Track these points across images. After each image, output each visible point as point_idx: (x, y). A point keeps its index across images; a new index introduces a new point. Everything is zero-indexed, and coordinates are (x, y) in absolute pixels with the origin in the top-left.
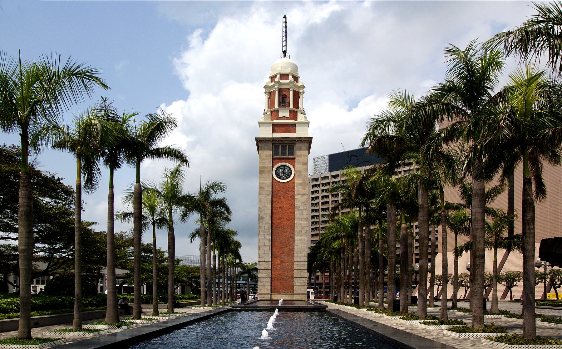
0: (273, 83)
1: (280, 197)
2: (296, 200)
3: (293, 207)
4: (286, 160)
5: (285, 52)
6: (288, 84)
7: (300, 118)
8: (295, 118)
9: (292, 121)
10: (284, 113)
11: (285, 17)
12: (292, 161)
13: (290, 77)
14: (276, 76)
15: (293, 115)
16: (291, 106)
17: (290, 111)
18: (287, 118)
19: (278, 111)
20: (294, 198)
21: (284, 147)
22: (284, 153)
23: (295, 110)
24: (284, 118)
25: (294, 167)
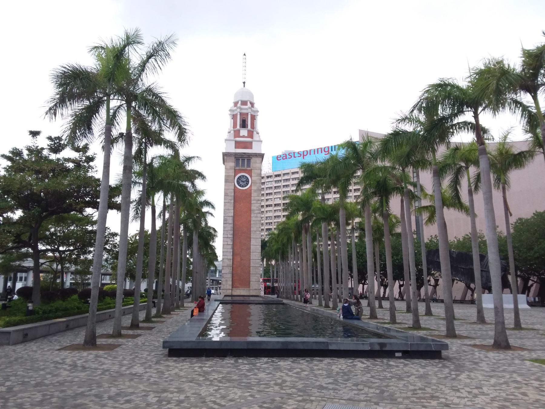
0: (236, 108)
1: (240, 202)
2: (252, 205)
3: (249, 211)
4: (245, 171)
5: (244, 83)
6: (246, 109)
7: (256, 137)
8: (252, 137)
9: (249, 139)
10: (244, 132)
11: (245, 55)
12: (250, 172)
13: (249, 103)
14: (238, 102)
15: (251, 134)
17: (249, 131)
19: (239, 131)
20: (251, 203)
22: (243, 165)
23: (252, 130)
24: (244, 137)
25: (251, 177)
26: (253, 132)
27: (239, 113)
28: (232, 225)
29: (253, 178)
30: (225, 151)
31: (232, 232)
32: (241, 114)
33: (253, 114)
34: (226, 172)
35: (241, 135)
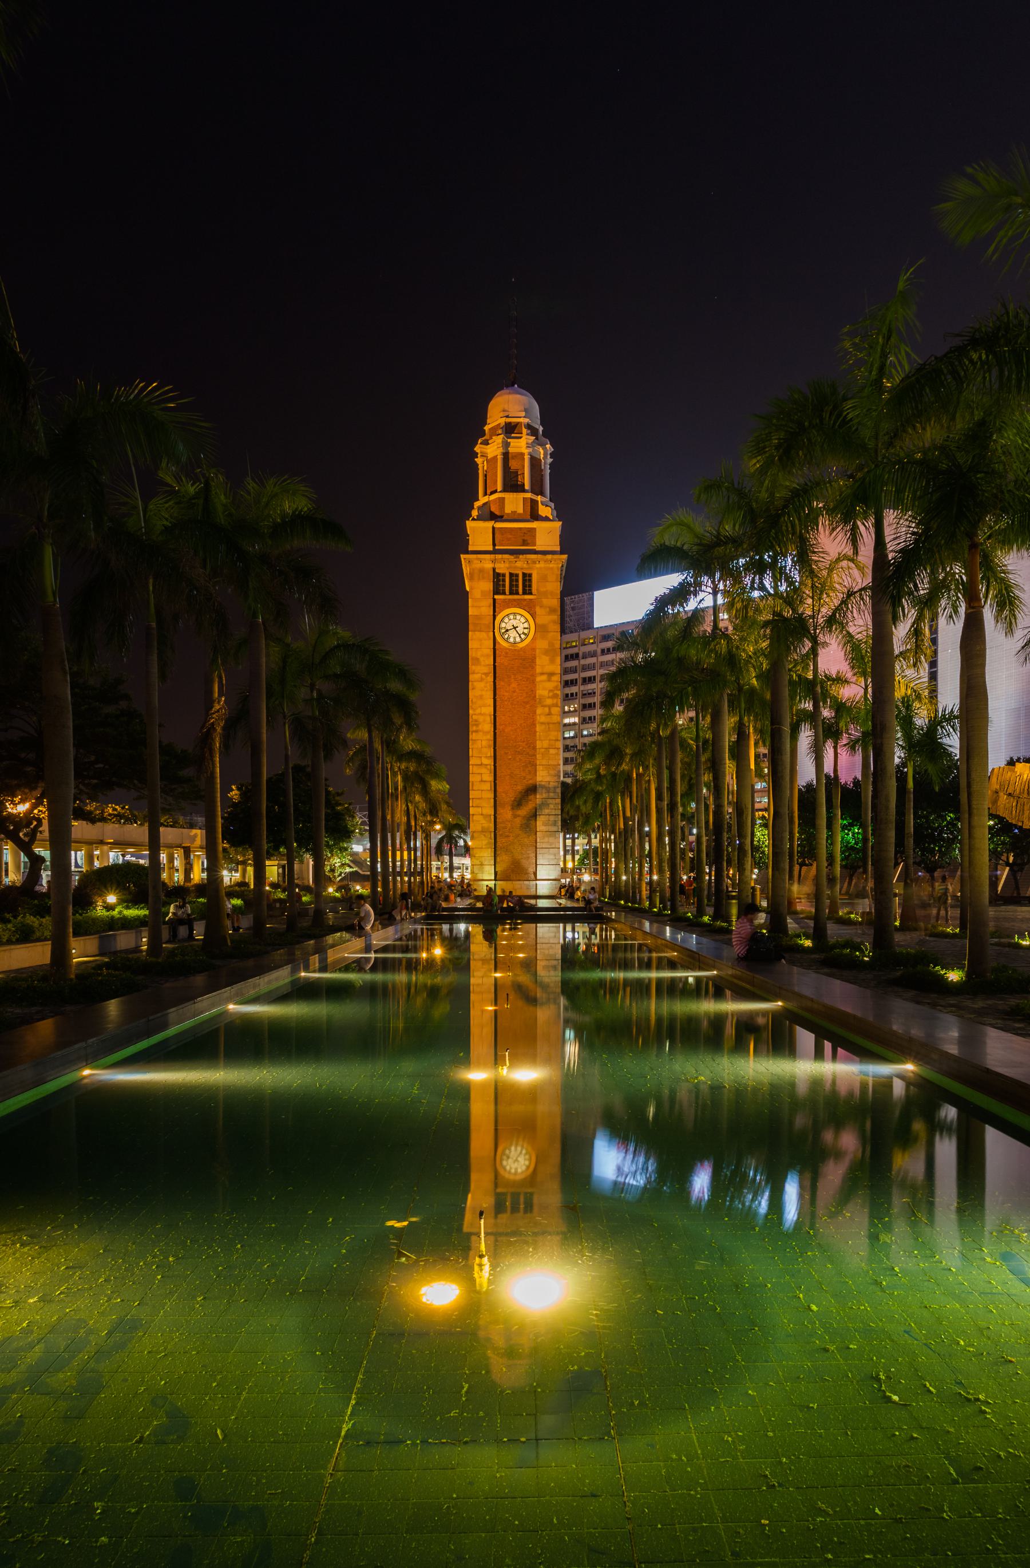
20: (534, 682)
28: (491, 736)
29: (539, 621)
31: (491, 753)
35: (508, 509)
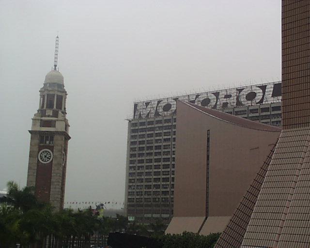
5: (55, 66)
10: (50, 112)
11: (58, 37)
16: (55, 107)
18: (52, 117)
19: (46, 110)
21: (47, 137)
23: (57, 110)
24: (49, 116)
25: (53, 152)
26: (58, 112)
27: (46, 95)
30: (30, 130)
32: (48, 95)
33: (59, 94)
34: (30, 148)
